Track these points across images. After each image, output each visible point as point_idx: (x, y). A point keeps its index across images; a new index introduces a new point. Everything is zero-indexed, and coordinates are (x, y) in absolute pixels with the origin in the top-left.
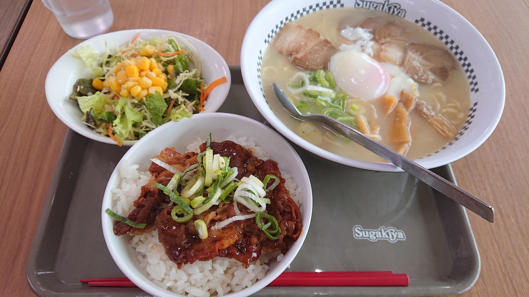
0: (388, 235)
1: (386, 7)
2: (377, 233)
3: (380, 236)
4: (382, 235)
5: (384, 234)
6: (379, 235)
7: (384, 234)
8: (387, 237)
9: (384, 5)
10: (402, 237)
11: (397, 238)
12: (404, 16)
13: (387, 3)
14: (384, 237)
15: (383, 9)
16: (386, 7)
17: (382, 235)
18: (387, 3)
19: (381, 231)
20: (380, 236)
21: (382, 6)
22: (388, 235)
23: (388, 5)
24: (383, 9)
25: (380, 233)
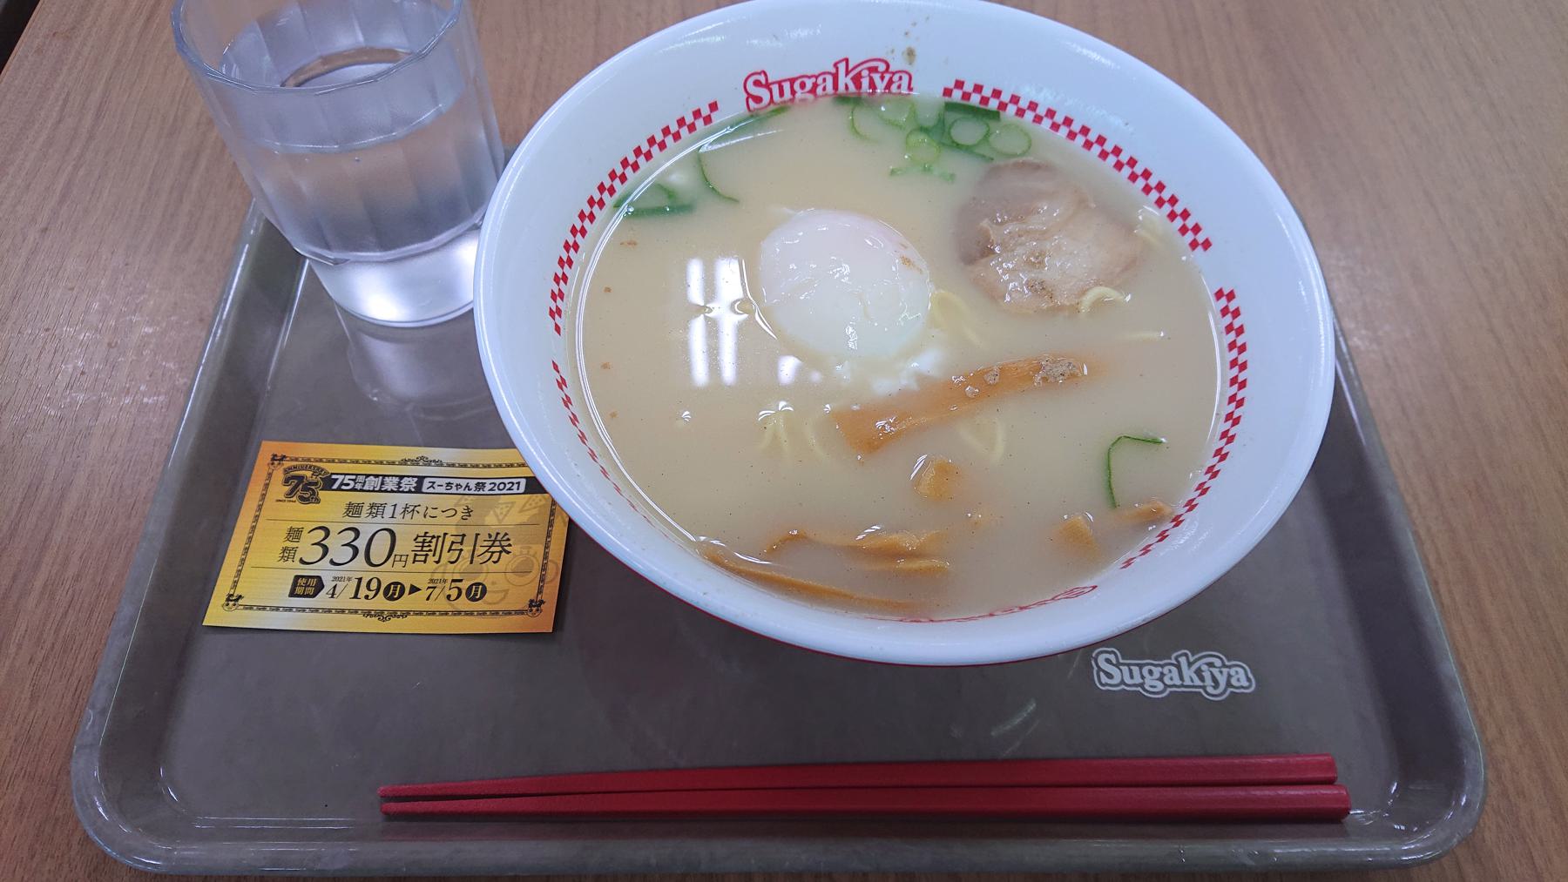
0: (1202, 679)
2: (1166, 670)
3: (1178, 682)
4: (1182, 678)
5: (1188, 673)
6: (1172, 677)
7: (1188, 673)
8: (1198, 682)
9: (835, 77)
10: (1246, 684)
11: (1229, 684)
12: (910, 88)
13: (842, 67)
14: (1187, 682)
15: (836, 86)
17: (1182, 678)
18: (842, 67)
19: (1178, 667)
20: (1178, 682)
21: (830, 79)
22: (1202, 679)
23: (847, 73)
24: (836, 86)
25: (1174, 669)
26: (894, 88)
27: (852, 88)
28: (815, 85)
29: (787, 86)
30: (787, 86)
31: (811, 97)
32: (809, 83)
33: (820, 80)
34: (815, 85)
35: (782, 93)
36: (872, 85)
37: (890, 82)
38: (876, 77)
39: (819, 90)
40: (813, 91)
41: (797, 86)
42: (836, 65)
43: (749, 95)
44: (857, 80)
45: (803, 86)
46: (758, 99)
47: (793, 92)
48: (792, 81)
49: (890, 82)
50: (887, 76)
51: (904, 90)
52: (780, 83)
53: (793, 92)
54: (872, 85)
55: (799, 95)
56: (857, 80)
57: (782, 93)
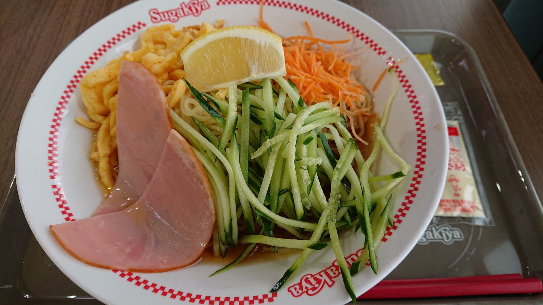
1: (186, 10)
9: (182, 9)
13: (183, 6)
16: (186, 10)
18: (183, 6)
21: (181, 11)
26: (204, 7)
27: (190, 12)
28: (176, 14)
29: (166, 14)
30: (166, 14)
31: (176, 18)
32: (174, 13)
33: (177, 11)
34: (176, 14)
35: (164, 16)
36: (197, 10)
37: (202, 6)
38: (196, 6)
39: (178, 15)
40: (176, 15)
41: (170, 14)
42: (181, 5)
43: (152, 17)
44: (190, 9)
45: (172, 13)
46: (156, 19)
47: (169, 16)
48: (167, 12)
49: (202, 6)
50: (199, 4)
51: (207, 6)
52: (163, 13)
53: (169, 16)
54: (197, 10)
55: (172, 17)
56: (190, 9)
57: (164, 16)
